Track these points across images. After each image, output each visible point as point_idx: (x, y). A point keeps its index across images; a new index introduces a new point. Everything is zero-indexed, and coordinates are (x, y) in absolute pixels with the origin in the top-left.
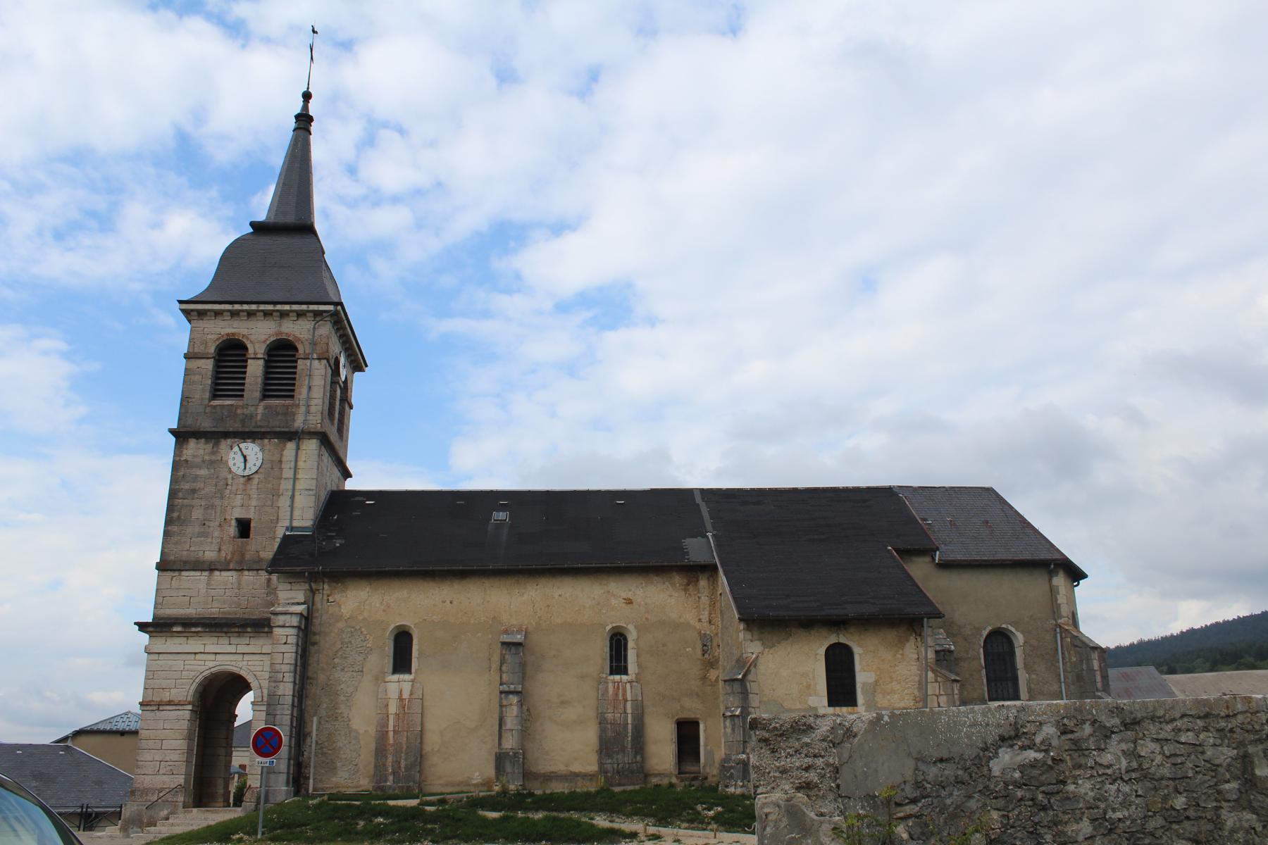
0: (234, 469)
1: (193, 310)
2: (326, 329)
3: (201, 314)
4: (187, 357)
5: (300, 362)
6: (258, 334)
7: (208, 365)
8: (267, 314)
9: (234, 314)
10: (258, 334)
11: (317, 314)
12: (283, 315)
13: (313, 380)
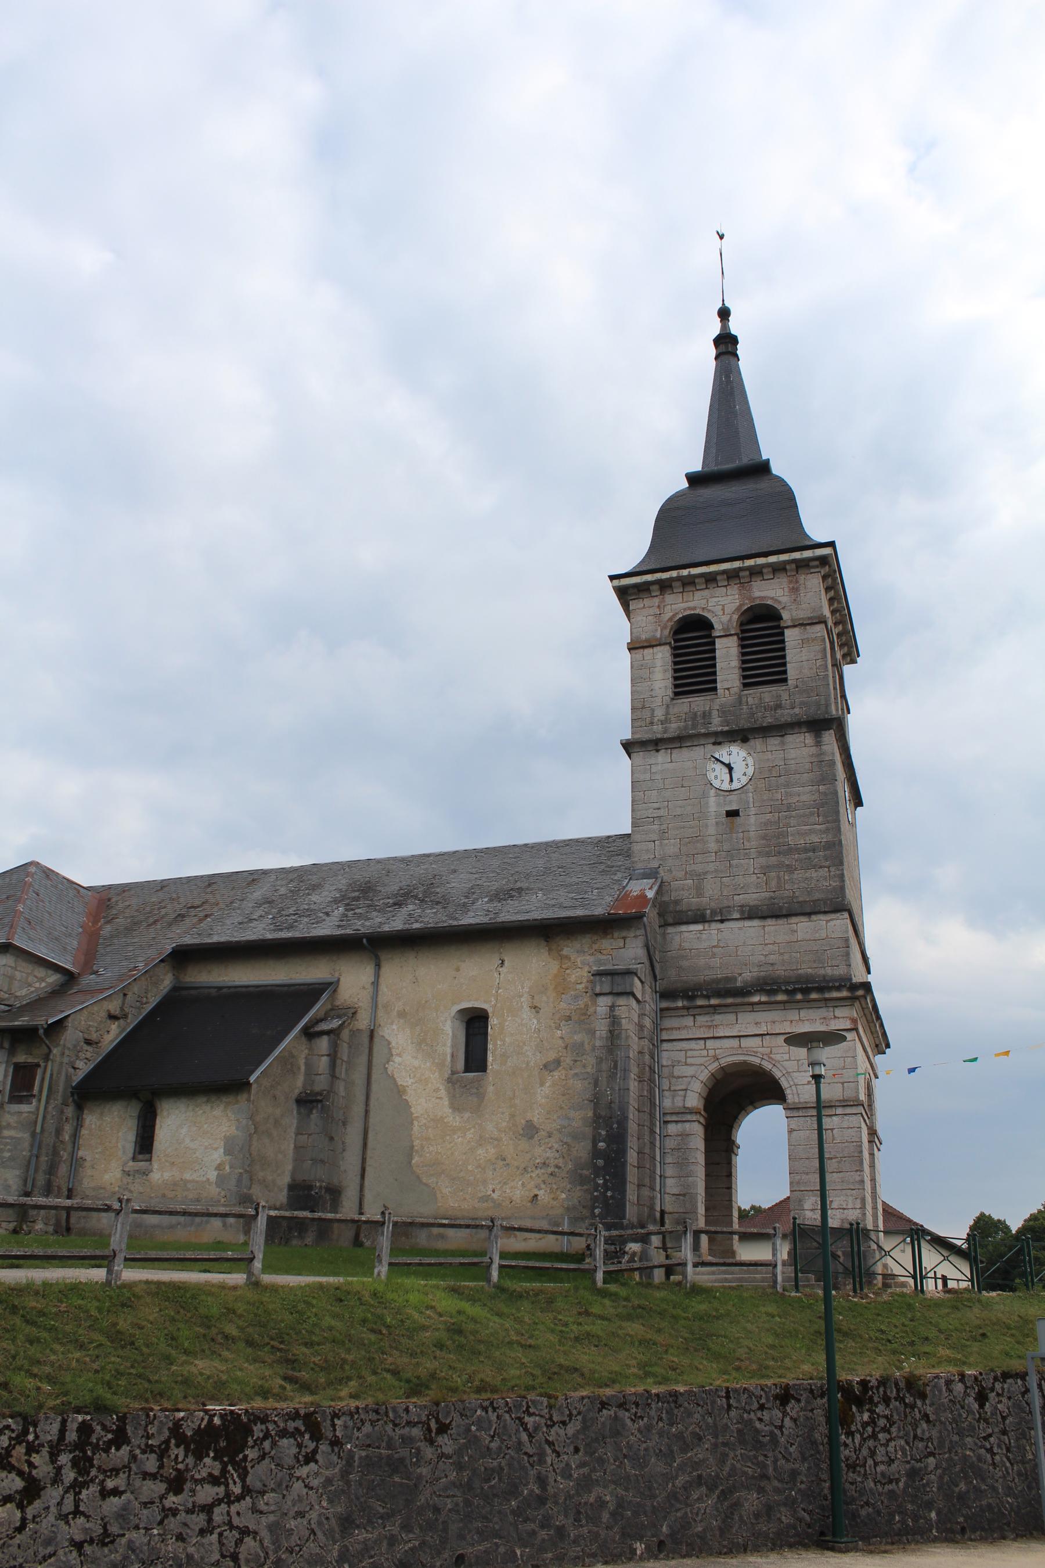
0: (716, 783)
1: (629, 591)
2: (813, 583)
3: (643, 589)
4: (631, 648)
5: (787, 632)
6: (722, 607)
7: (662, 658)
8: (732, 576)
9: (688, 583)
10: (722, 607)
11: (802, 565)
12: (756, 572)
13: (801, 653)
